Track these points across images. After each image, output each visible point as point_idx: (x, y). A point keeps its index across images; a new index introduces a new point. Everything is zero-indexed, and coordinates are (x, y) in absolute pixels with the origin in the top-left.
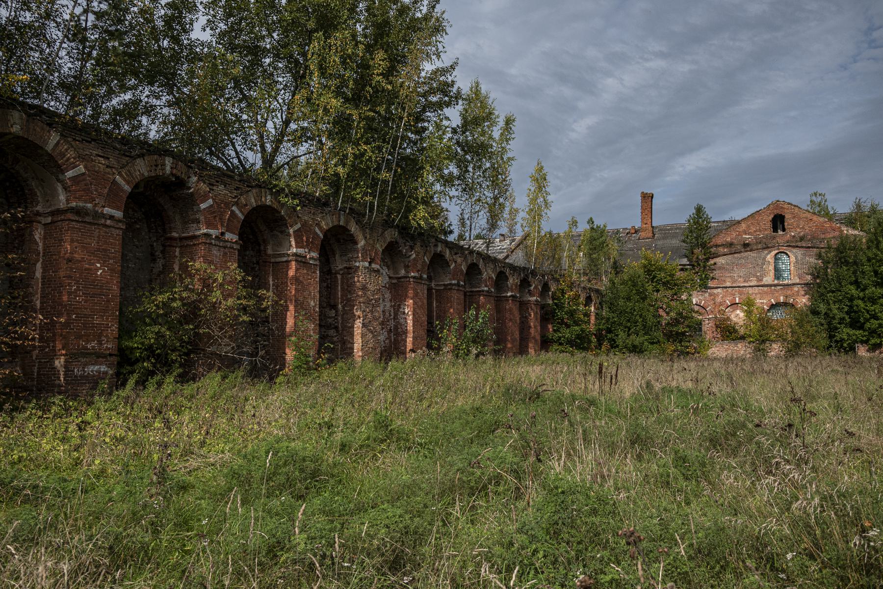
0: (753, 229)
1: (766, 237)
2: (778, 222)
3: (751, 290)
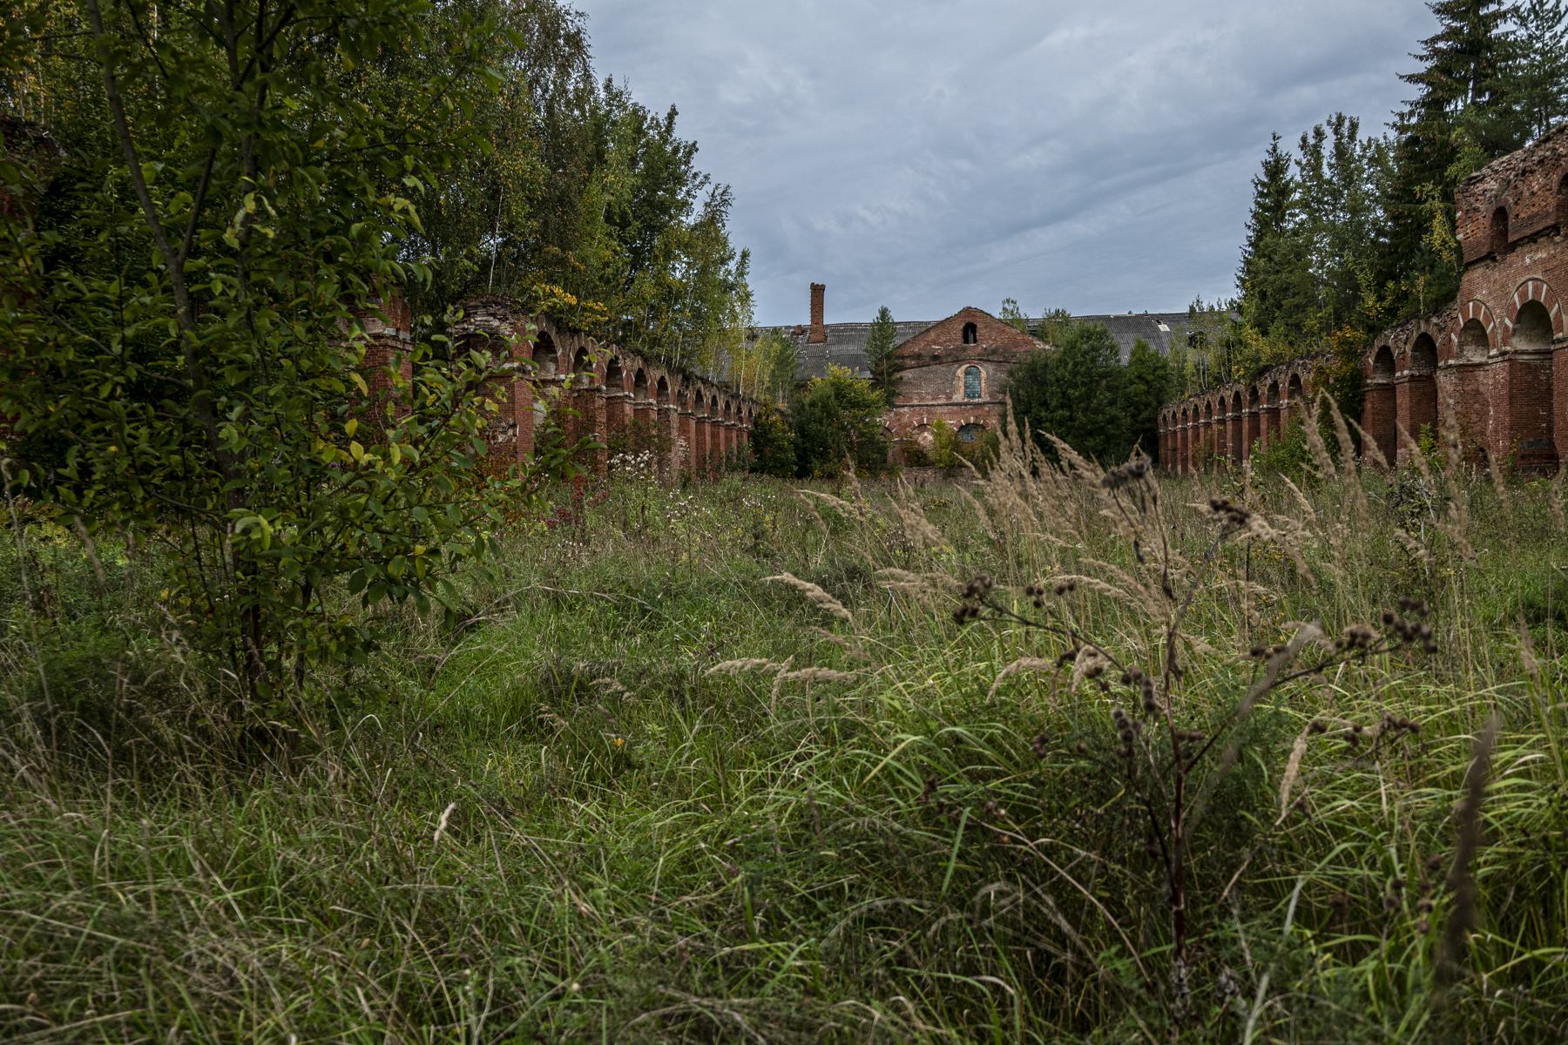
0: (943, 339)
1: (956, 349)
2: (970, 331)
3: (939, 410)
